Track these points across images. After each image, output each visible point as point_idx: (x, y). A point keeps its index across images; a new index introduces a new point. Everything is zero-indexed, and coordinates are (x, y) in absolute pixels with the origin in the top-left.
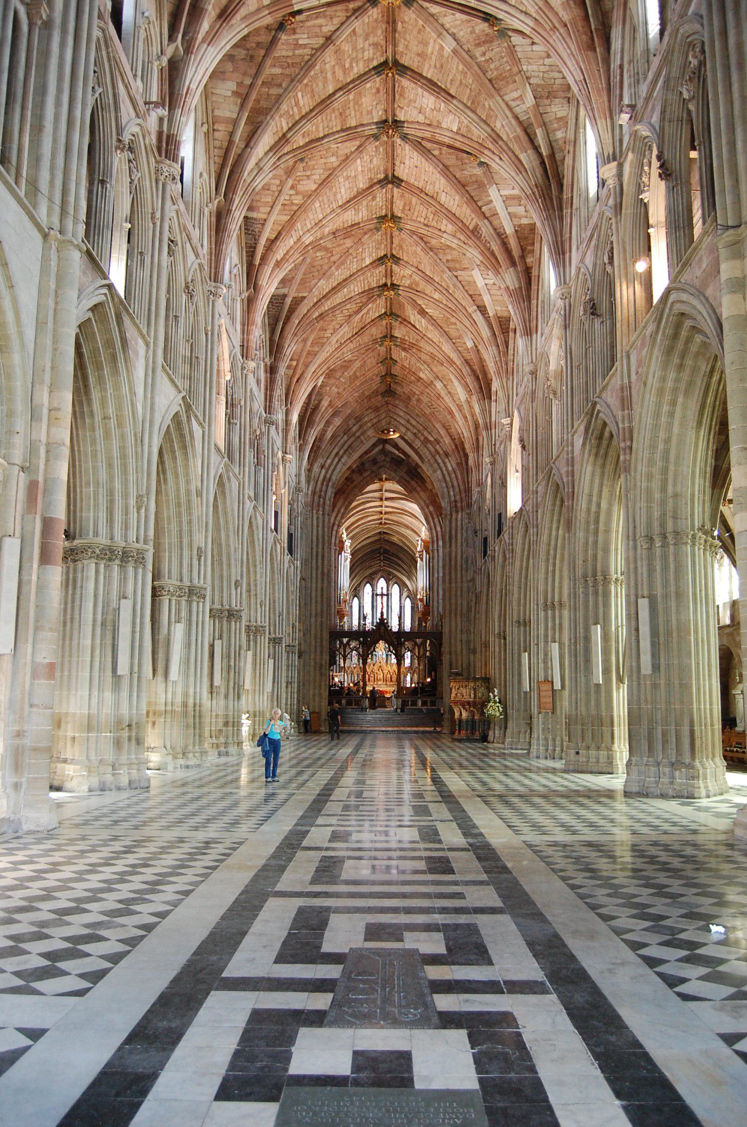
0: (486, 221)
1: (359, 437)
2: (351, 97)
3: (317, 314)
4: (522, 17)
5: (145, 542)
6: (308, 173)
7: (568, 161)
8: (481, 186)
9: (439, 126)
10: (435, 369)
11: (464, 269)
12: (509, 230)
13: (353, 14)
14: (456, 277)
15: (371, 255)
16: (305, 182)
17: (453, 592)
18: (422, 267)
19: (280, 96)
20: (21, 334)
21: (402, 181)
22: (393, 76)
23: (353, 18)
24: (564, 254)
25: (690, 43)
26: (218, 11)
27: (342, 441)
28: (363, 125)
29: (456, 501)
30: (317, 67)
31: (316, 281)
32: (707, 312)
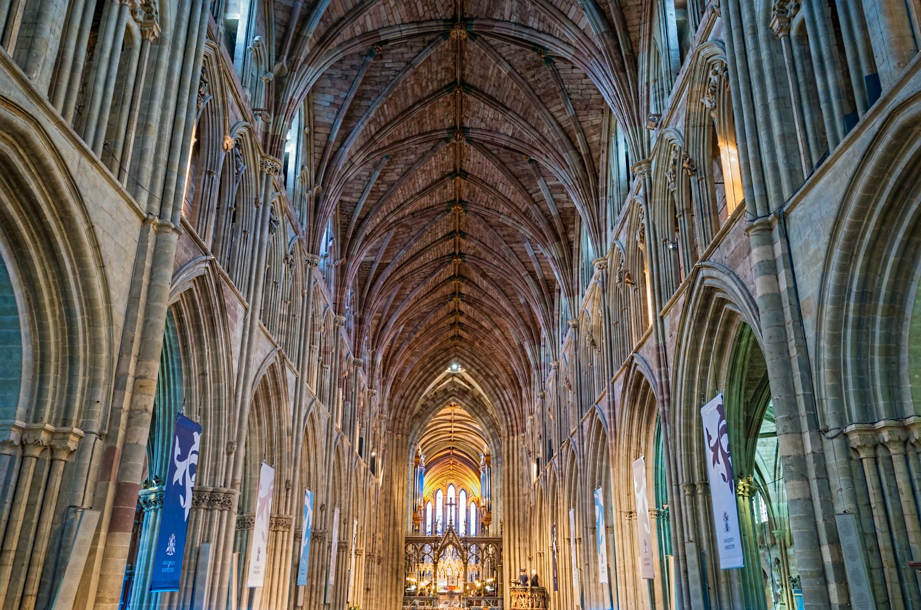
0: (535, 205)
2: (427, 109)
3: (398, 277)
4: (565, 47)
5: (233, 486)
6: (392, 167)
7: (603, 158)
8: (531, 178)
9: (497, 131)
10: (494, 319)
11: (518, 242)
12: (554, 213)
13: (429, 44)
14: (511, 248)
15: (442, 231)
16: (390, 174)
18: (484, 240)
19: (369, 106)
20: (109, 309)
21: (468, 174)
22: (461, 93)
23: (429, 47)
24: (600, 232)
25: (709, 64)
26: (318, 38)
28: (436, 131)
30: (400, 85)
31: (398, 251)
32: (739, 288)
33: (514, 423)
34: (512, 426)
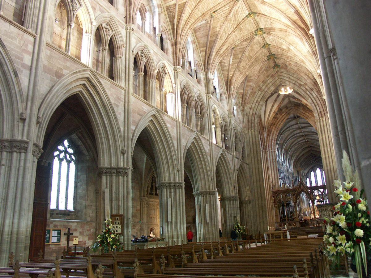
1: (266, 91)
17: (327, 160)
27: (258, 95)
29: (321, 112)
33: (322, 110)
34: (321, 112)
